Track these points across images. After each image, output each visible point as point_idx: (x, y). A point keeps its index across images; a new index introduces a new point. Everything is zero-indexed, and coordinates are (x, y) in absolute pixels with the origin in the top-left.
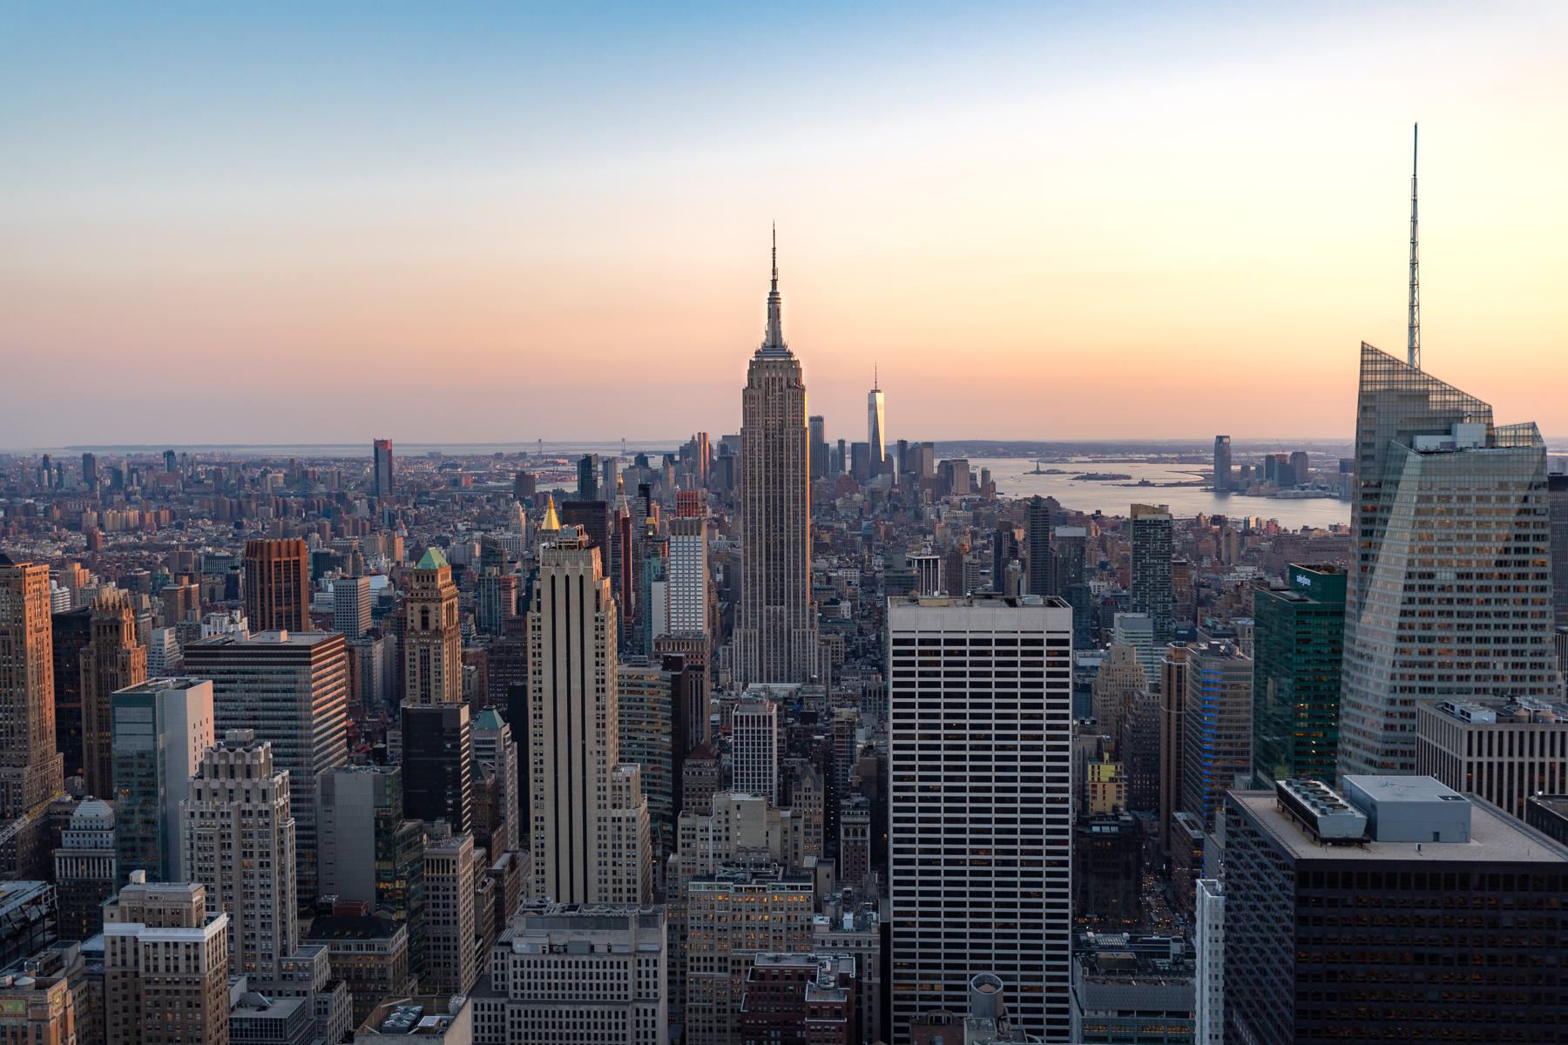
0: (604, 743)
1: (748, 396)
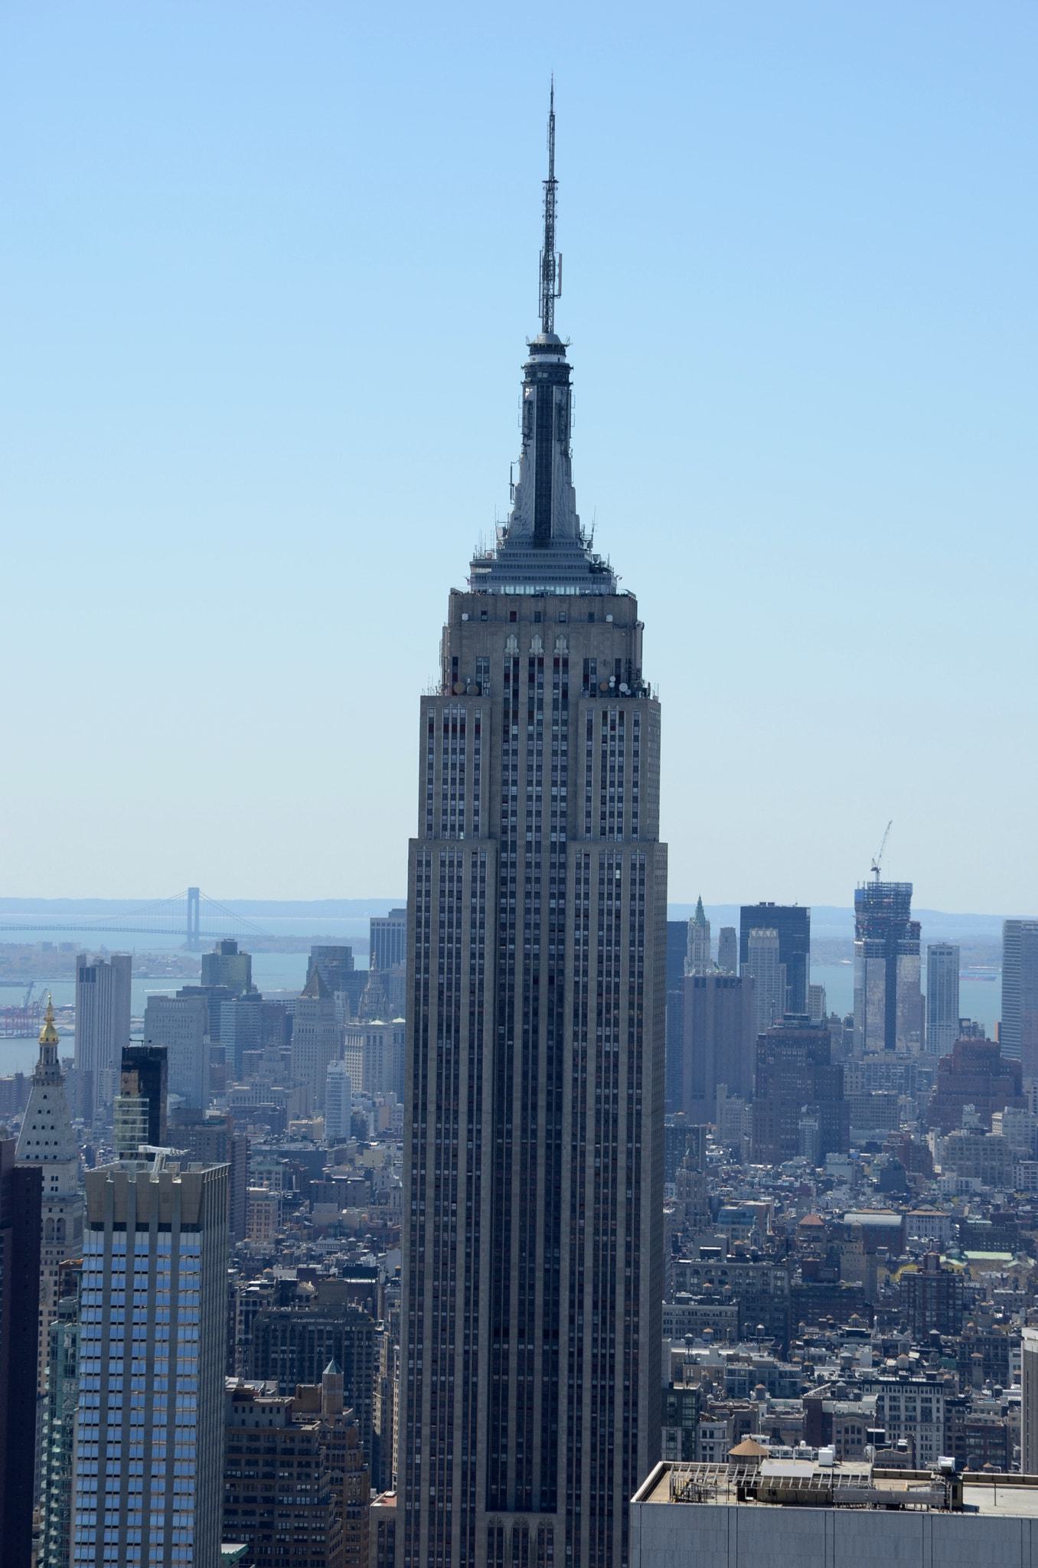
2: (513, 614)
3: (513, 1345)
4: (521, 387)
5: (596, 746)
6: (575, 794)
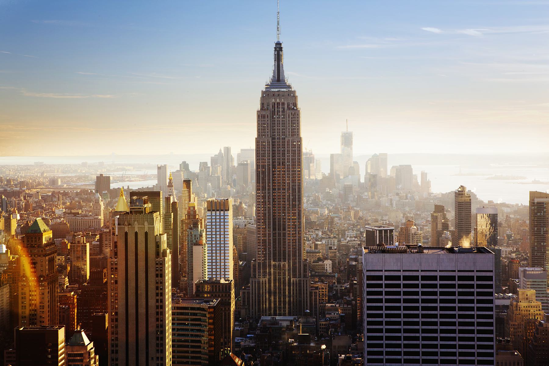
1: (261, 117)
2: (274, 94)
3: (277, 232)
4: (274, 52)
5: (290, 119)
6: (286, 128)
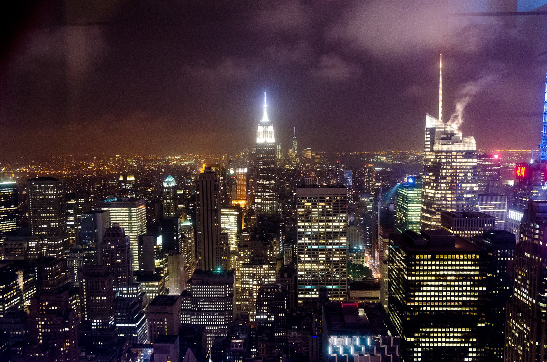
0: (217, 227)
